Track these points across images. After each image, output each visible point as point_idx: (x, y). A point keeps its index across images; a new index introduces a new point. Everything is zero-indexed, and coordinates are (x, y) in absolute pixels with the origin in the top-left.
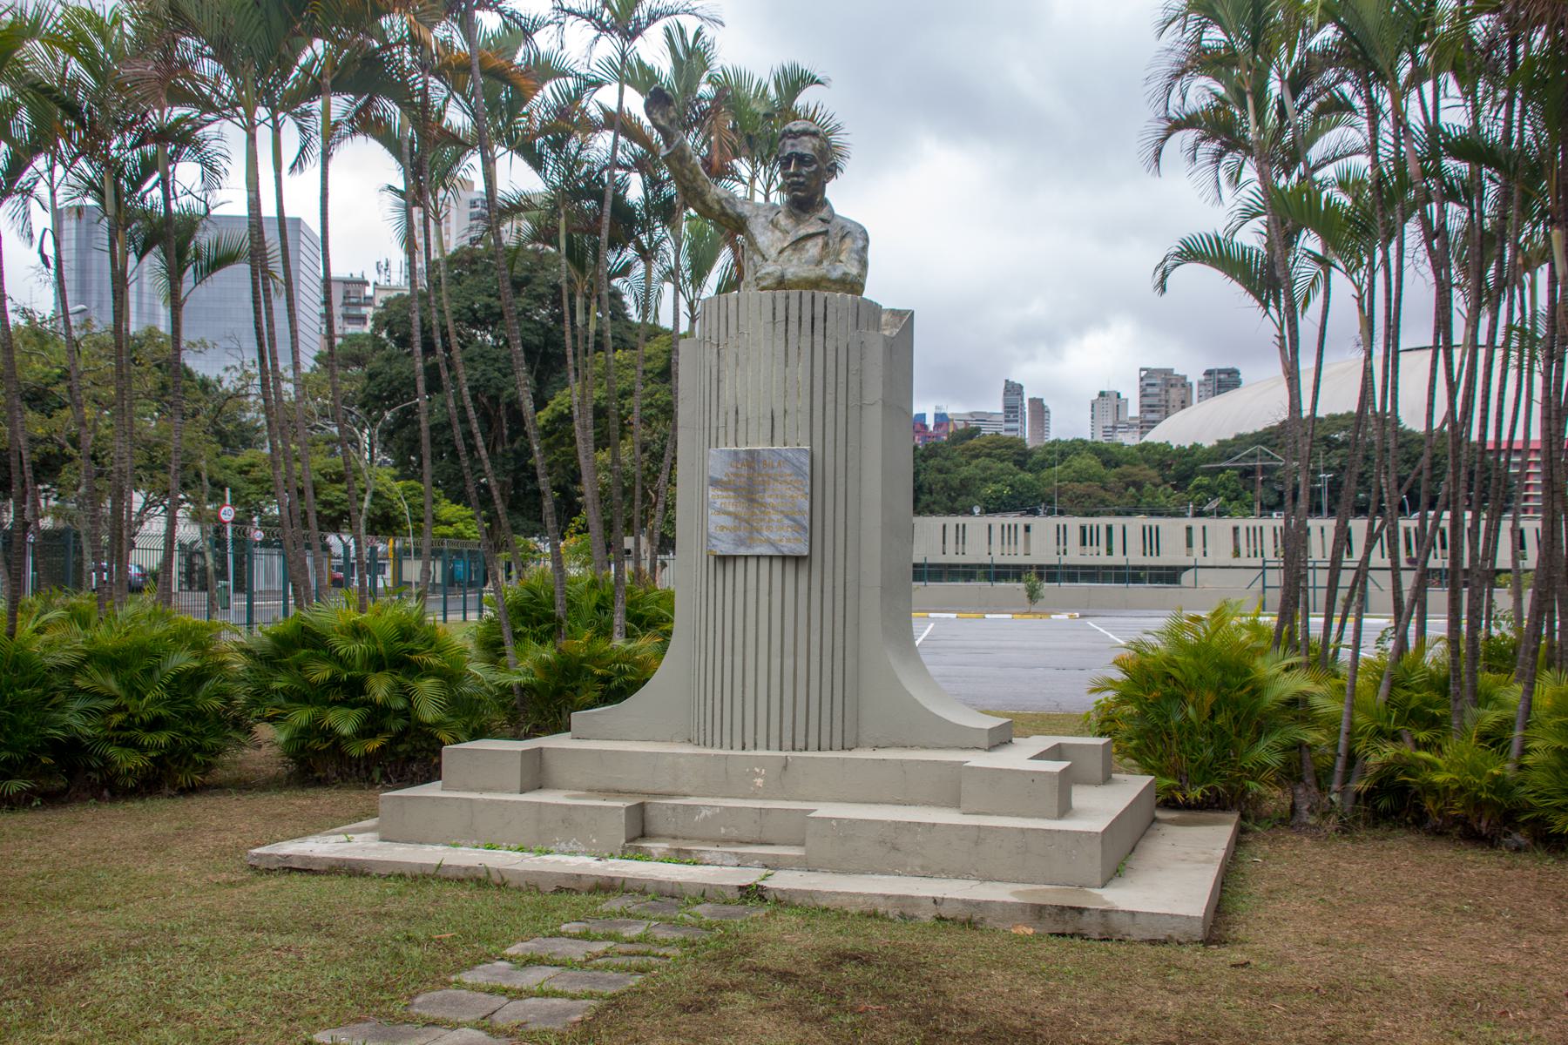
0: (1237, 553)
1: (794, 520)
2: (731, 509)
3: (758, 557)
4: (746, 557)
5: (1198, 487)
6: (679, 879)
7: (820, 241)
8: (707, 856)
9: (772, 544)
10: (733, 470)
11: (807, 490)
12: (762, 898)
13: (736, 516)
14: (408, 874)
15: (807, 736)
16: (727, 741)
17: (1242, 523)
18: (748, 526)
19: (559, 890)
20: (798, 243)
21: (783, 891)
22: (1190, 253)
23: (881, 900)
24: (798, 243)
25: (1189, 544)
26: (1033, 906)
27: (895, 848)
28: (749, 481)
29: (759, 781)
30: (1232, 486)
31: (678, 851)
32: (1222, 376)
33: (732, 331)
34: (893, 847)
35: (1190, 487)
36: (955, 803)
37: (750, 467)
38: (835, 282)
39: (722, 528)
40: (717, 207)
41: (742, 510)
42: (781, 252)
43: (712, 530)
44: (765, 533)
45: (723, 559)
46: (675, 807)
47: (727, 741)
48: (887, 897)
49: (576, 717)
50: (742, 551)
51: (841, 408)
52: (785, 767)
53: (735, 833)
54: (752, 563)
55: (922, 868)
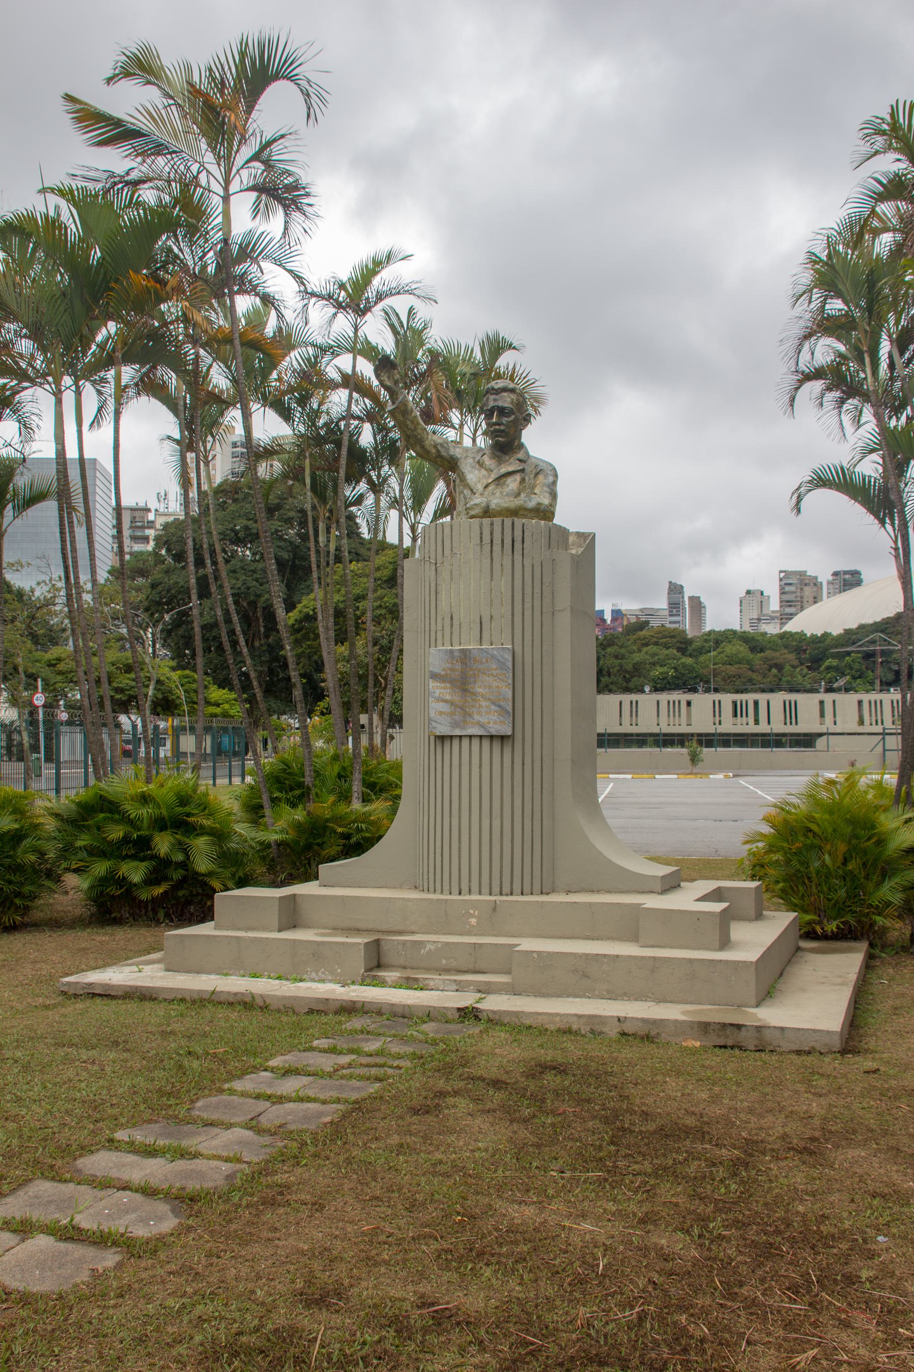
0: (861, 722)
1: (500, 706)
2: (448, 697)
3: (470, 737)
4: (461, 737)
5: (829, 668)
6: (409, 1002)
7: (518, 477)
8: (432, 983)
9: (482, 726)
10: (448, 665)
11: (510, 681)
12: (477, 1018)
13: (452, 703)
14: (188, 998)
15: (512, 883)
16: (446, 888)
17: (866, 697)
18: (462, 711)
19: (311, 1012)
20: (500, 479)
21: (494, 1012)
22: (820, 481)
23: (575, 1019)
24: (500, 479)
25: (822, 715)
26: (700, 1023)
27: (586, 976)
28: (462, 675)
29: (473, 921)
30: (856, 666)
31: (408, 979)
32: (847, 577)
33: (447, 552)
34: (584, 976)
35: (822, 668)
36: (634, 937)
37: (462, 663)
38: (531, 510)
39: (441, 713)
40: (433, 451)
41: (457, 698)
42: (486, 487)
43: (432, 715)
44: (476, 717)
45: (442, 738)
46: (404, 943)
47: (446, 888)
48: (579, 1017)
49: (323, 869)
50: (457, 732)
51: (537, 614)
52: (494, 909)
53: (454, 964)
54: (465, 742)
55: (608, 992)
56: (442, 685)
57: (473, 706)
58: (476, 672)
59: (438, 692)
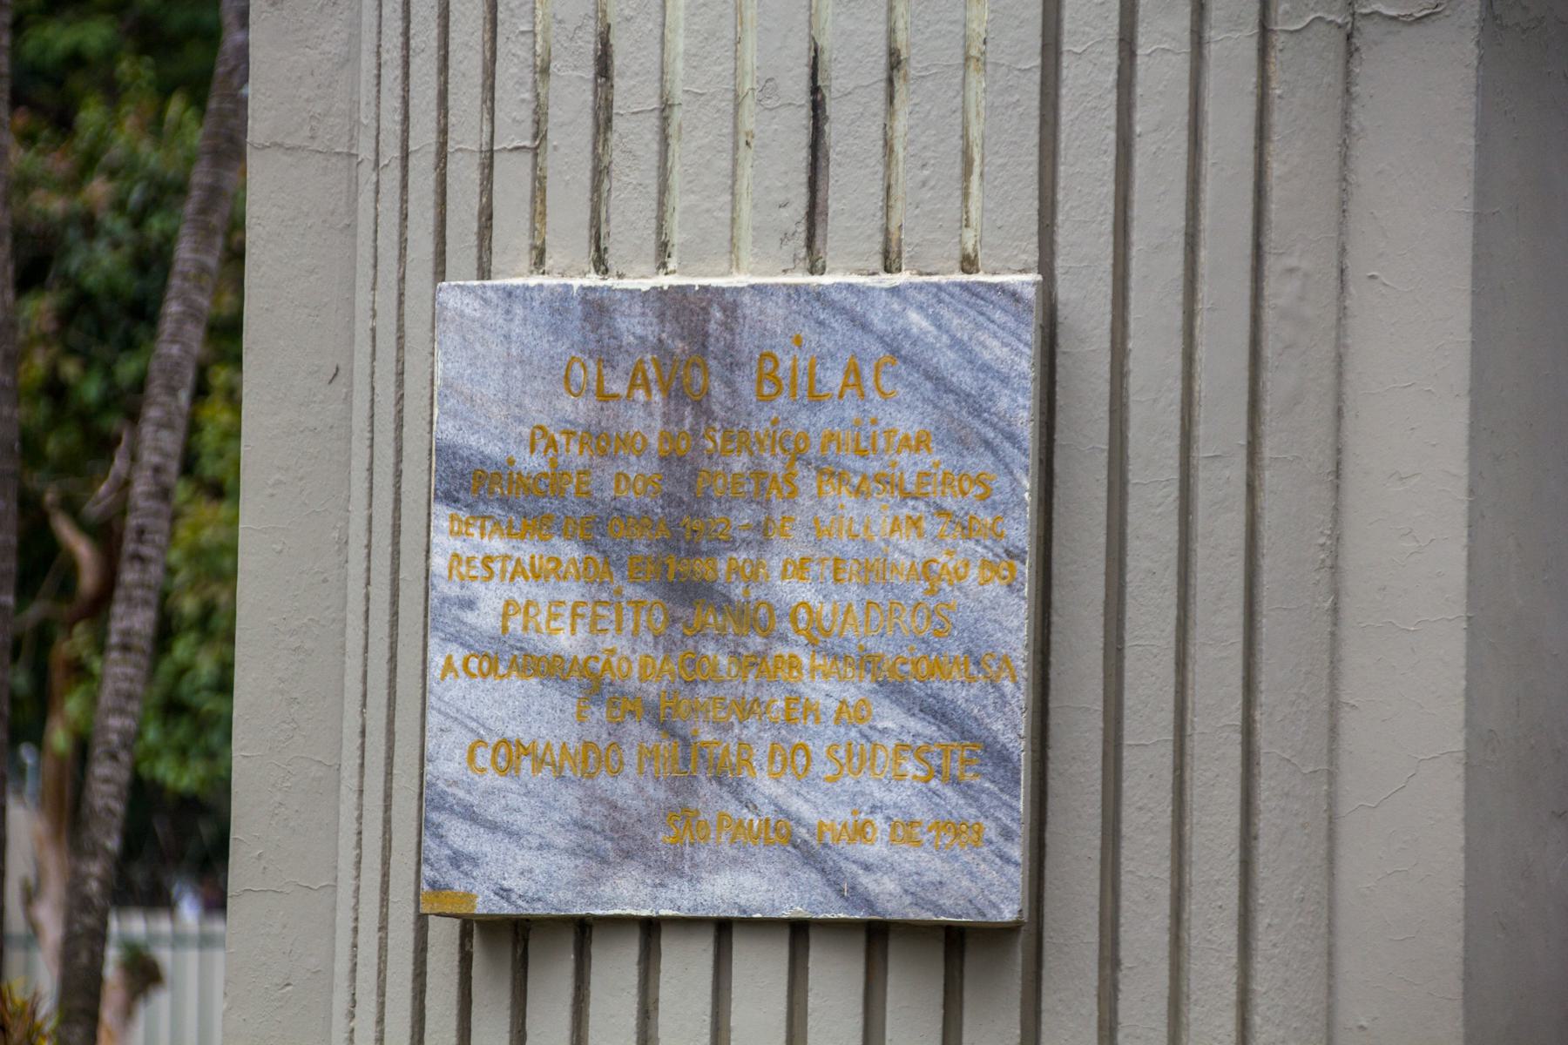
2: (566, 640)
9: (807, 852)
13: (593, 685)
18: (666, 742)
39: (511, 755)
41: (631, 649)
56: (527, 550)
57: (748, 709)
58: (775, 464)
59: (491, 598)
